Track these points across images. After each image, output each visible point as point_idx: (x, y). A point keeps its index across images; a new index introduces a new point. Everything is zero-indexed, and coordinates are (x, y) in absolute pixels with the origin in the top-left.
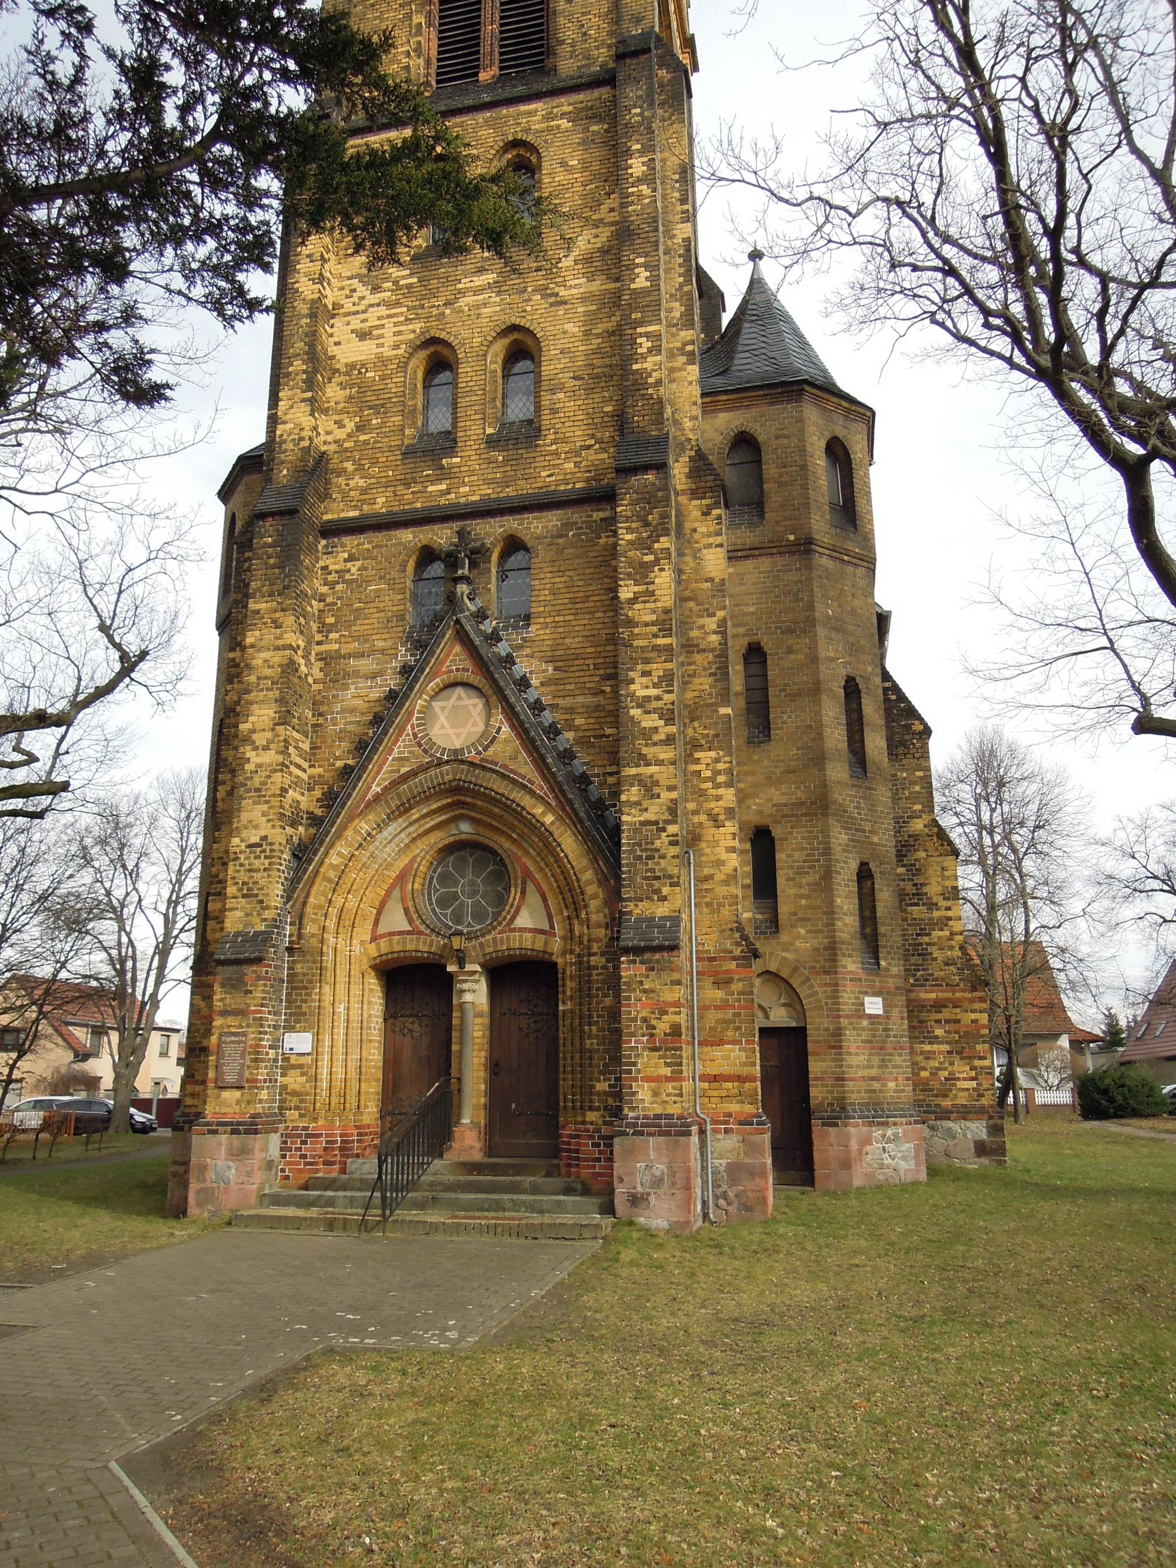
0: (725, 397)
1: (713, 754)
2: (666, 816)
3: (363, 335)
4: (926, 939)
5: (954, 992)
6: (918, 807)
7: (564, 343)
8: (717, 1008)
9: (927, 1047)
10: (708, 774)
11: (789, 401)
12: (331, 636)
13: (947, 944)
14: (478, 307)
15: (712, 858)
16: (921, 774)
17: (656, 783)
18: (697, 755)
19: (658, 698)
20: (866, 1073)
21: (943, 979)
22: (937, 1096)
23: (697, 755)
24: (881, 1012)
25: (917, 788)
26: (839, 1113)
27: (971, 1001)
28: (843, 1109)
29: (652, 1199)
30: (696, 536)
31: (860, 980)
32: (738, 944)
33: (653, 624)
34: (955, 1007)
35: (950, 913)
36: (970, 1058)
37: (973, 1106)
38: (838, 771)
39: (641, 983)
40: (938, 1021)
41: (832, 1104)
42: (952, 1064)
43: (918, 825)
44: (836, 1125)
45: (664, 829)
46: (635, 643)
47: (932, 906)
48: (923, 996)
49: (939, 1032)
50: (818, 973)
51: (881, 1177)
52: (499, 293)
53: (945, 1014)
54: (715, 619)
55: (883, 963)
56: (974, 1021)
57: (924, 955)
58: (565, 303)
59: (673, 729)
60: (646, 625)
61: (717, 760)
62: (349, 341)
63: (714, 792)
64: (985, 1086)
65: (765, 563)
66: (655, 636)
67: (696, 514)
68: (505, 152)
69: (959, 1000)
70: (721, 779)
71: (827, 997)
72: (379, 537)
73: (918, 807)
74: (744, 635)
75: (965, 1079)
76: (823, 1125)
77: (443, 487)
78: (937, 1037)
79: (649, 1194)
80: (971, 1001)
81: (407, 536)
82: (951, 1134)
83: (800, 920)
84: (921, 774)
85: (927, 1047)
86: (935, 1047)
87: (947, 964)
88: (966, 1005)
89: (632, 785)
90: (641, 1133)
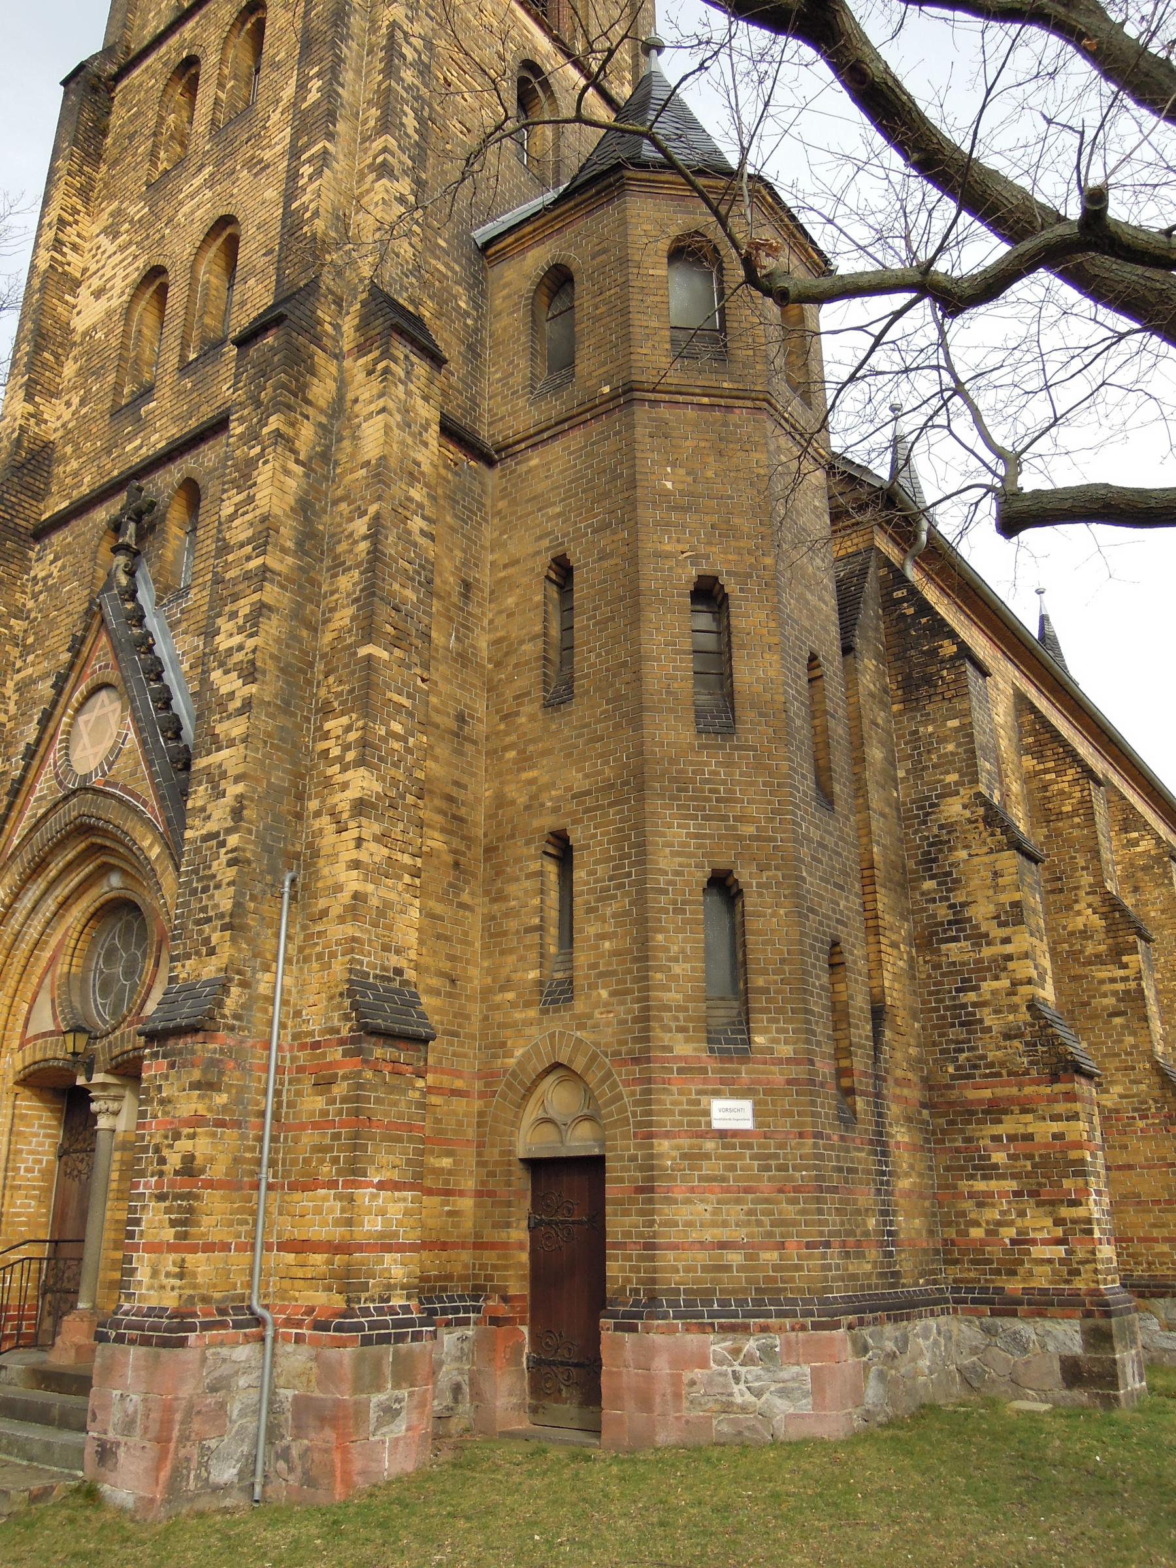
0: (529, 228)
1: (345, 720)
2: (230, 823)
3: (98, 294)
4: (972, 996)
5: (1021, 1086)
6: (952, 778)
7: (263, 215)
8: (315, 1126)
9: (980, 1186)
10: (335, 752)
11: (610, 201)
12: (30, 658)
13: (1006, 1001)
14: (193, 212)
15: (330, 882)
16: (955, 723)
17: (223, 775)
18: (327, 726)
19: (240, 648)
20: (709, 1235)
21: (1002, 1064)
22: (997, 1272)
23: (327, 726)
24: (748, 1124)
25: (951, 747)
26: (649, 1304)
27: (1052, 1100)
28: (653, 1300)
29: (121, 1452)
30: (357, 408)
31: (704, 1071)
32: (347, 1018)
33: (249, 541)
34: (1024, 1111)
35: (1009, 949)
36: (1052, 1203)
37: (1059, 1292)
38: (672, 732)
39: (159, 1088)
40: (996, 1139)
41: (636, 1291)
42: (1022, 1214)
43: (954, 809)
44: (633, 1329)
45: (222, 844)
46: (228, 576)
47: (980, 938)
48: (971, 1094)
49: (999, 1157)
50: (624, 1062)
51: (725, 1428)
52: (211, 187)
53: (1006, 1127)
54: (366, 518)
55: (759, 1039)
56: (1057, 1136)
57: (971, 1024)
58: (268, 166)
59: (253, 689)
60: (242, 545)
61: (348, 729)
62: (87, 306)
63: (340, 778)
64: (1081, 1255)
65: (577, 438)
66: (249, 558)
67: (361, 376)
68: (243, 24)
69: (1030, 1099)
70: (351, 756)
71: (637, 1103)
72: (78, 525)
73: (952, 778)
74: (548, 549)
75: (1045, 1242)
76: (618, 1327)
77: (139, 441)
78: (995, 1166)
79: (118, 1444)
80: (1052, 1100)
81: (102, 515)
82: (1018, 1343)
83: (601, 975)
84: (955, 723)
85: (980, 1186)
86: (994, 1185)
87: (1007, 1037)
88: (1042, 1108)
89: (200, 784)
90: (120, 1339)
